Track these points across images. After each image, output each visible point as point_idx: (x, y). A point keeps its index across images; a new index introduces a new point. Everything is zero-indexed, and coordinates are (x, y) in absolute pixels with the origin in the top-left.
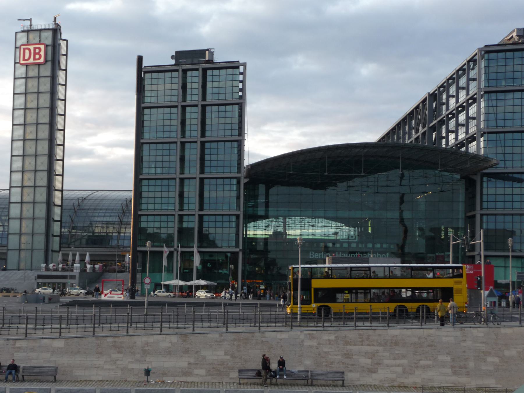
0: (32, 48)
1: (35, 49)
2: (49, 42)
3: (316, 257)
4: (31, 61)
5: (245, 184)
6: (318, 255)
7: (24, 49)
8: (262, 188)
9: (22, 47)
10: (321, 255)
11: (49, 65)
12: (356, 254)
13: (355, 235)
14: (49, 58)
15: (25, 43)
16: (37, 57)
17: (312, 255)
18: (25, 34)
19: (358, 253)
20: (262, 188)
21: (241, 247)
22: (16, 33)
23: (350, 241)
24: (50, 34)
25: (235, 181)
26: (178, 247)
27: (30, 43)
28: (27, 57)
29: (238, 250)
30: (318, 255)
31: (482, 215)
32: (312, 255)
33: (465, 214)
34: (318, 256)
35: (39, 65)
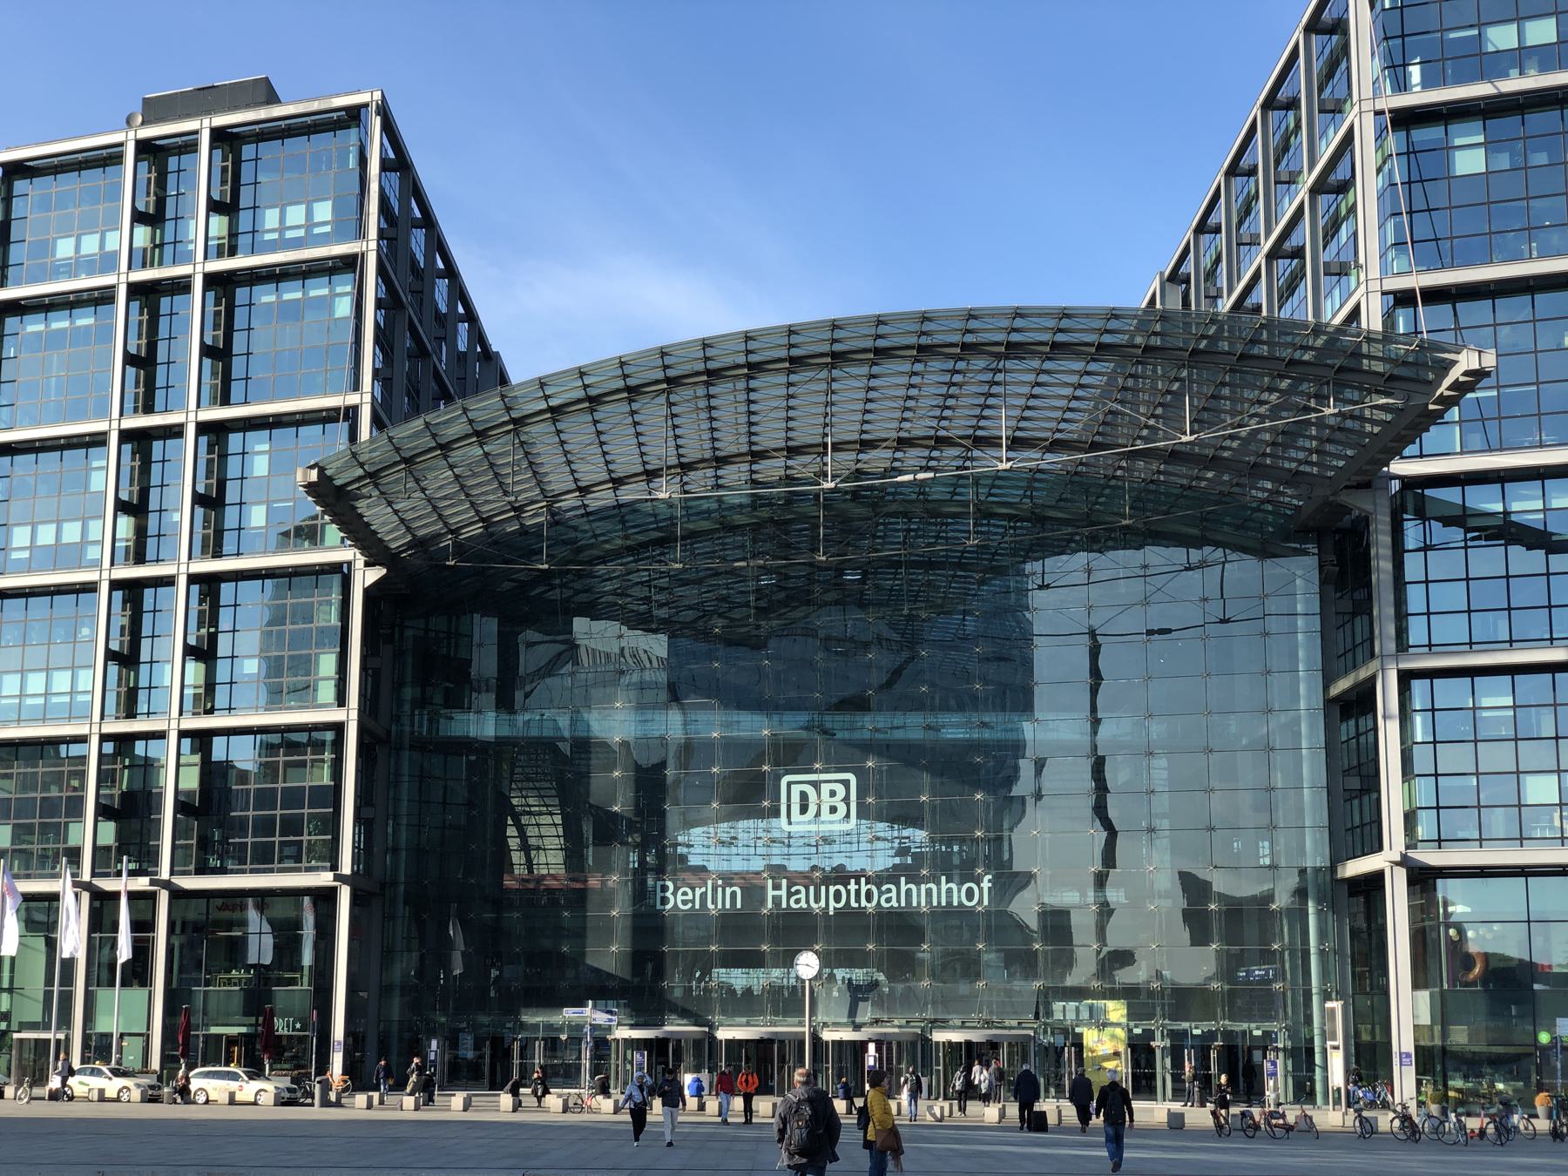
3: (685, 902)
5: (367, 591)
6: (690, 897)
8: (486, 628)
10: (704, 896)
12: (853, 887)
13: (846, 800)
19: (858, 883)
20: (486, 628)
21: (346, 868)
23: (823, 828)
29: (325, 879)
31: (1406, 678)
32: (669, 894)
33: (1326, 688)
34: (693, 901)
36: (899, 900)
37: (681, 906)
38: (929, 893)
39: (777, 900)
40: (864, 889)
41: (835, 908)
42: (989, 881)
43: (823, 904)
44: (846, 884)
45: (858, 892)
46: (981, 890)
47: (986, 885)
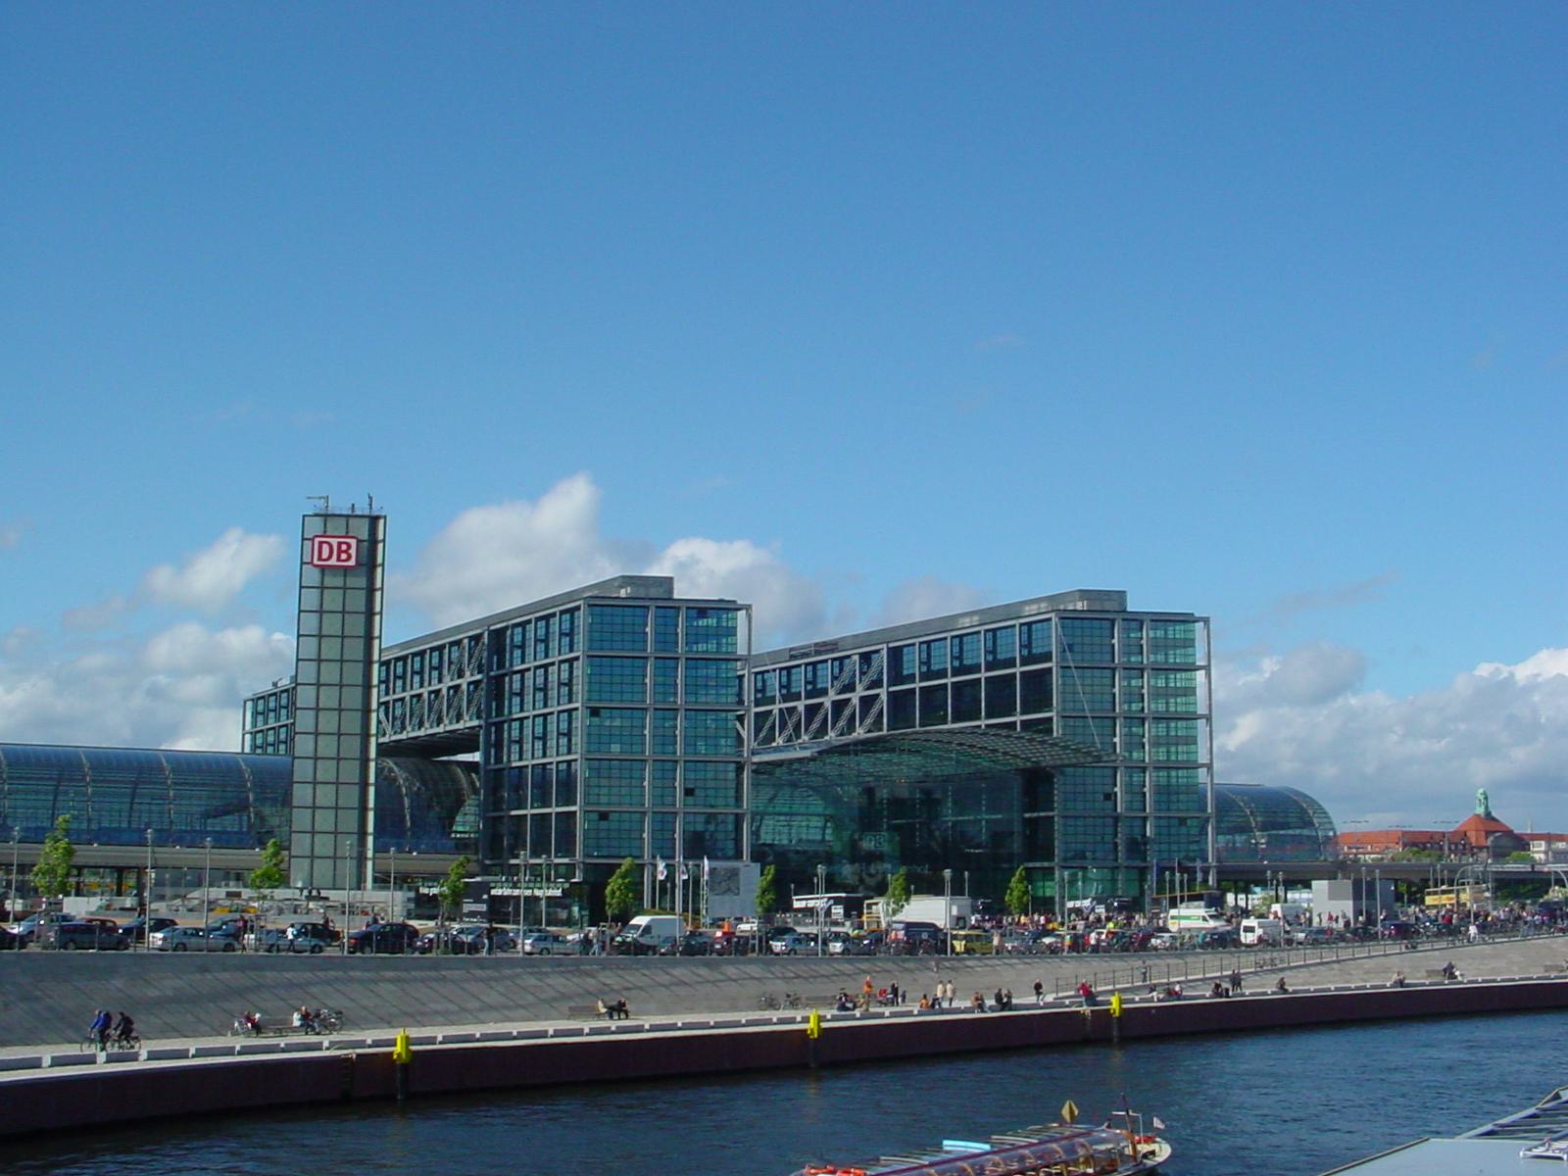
0: (334, 542)
1: (340, 544)
2: (365, 536)
4: (333, 562)
7: (321, 543)
9: (317, 540)
11: (364, 569)
14: (364, 560)
15: (322, 534)
16: (344, 556)
18: (319, 521)
22: (304, 516)
24: (366, 523)
25: (733, 766)
26: (654, 857)
27: (328, 534)
28: (325, 555)
35: (346, 568)
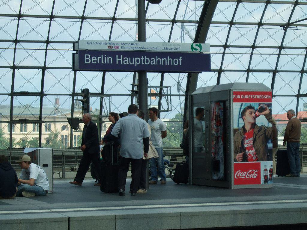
3: (94, 61)
12: (142, 58)
17: (89, 59)
19: (144, 57)
30: (96, 60)
32: (89, 59)
36: (156, 63)
37: (93, 62)
38: (164, 61)
39: (119, 61)
40: (145, 59)
41: (137, 65)
42: (181, 58)
43: (133, 63)
44: (140, 57)
45: (144, 60)
46: (179, 61)
47: (180, 59)
